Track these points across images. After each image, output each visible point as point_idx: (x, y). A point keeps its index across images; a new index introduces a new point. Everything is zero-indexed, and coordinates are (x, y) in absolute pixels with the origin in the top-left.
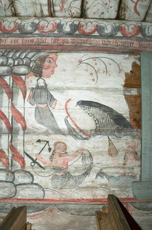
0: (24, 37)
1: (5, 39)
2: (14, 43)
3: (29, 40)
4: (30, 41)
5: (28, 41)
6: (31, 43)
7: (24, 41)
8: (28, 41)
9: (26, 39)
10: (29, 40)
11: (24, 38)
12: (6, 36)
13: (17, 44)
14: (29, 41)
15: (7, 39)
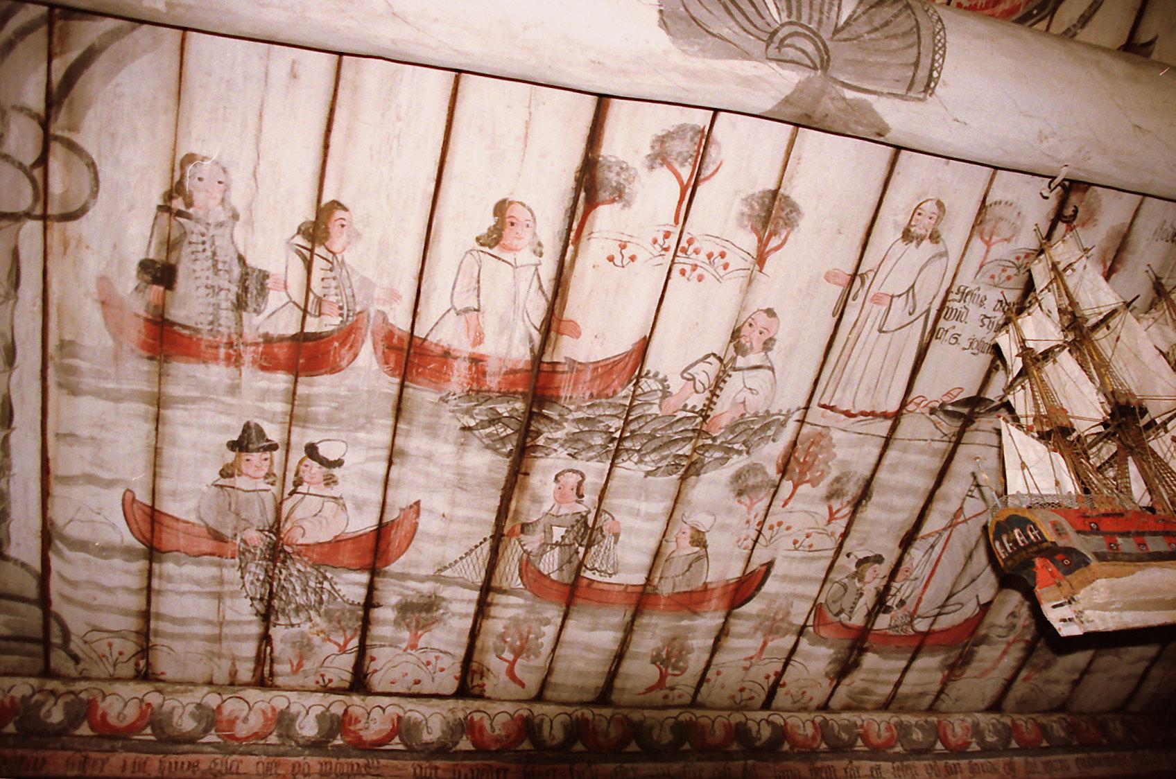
0: (166, 753)
1: (104, 756)
2: (133, 772)
3: (183, 763)
4: (186, 766)
5: (179, 764)
6: (189, 774)
7: (167, 765)
8: (179, 764)
9: (173, 758)
10: (183, 763)
11: (169, 756)
12: (107, 745)
13: (141, 775)
14: (182, 767)
15: (108, 759)
